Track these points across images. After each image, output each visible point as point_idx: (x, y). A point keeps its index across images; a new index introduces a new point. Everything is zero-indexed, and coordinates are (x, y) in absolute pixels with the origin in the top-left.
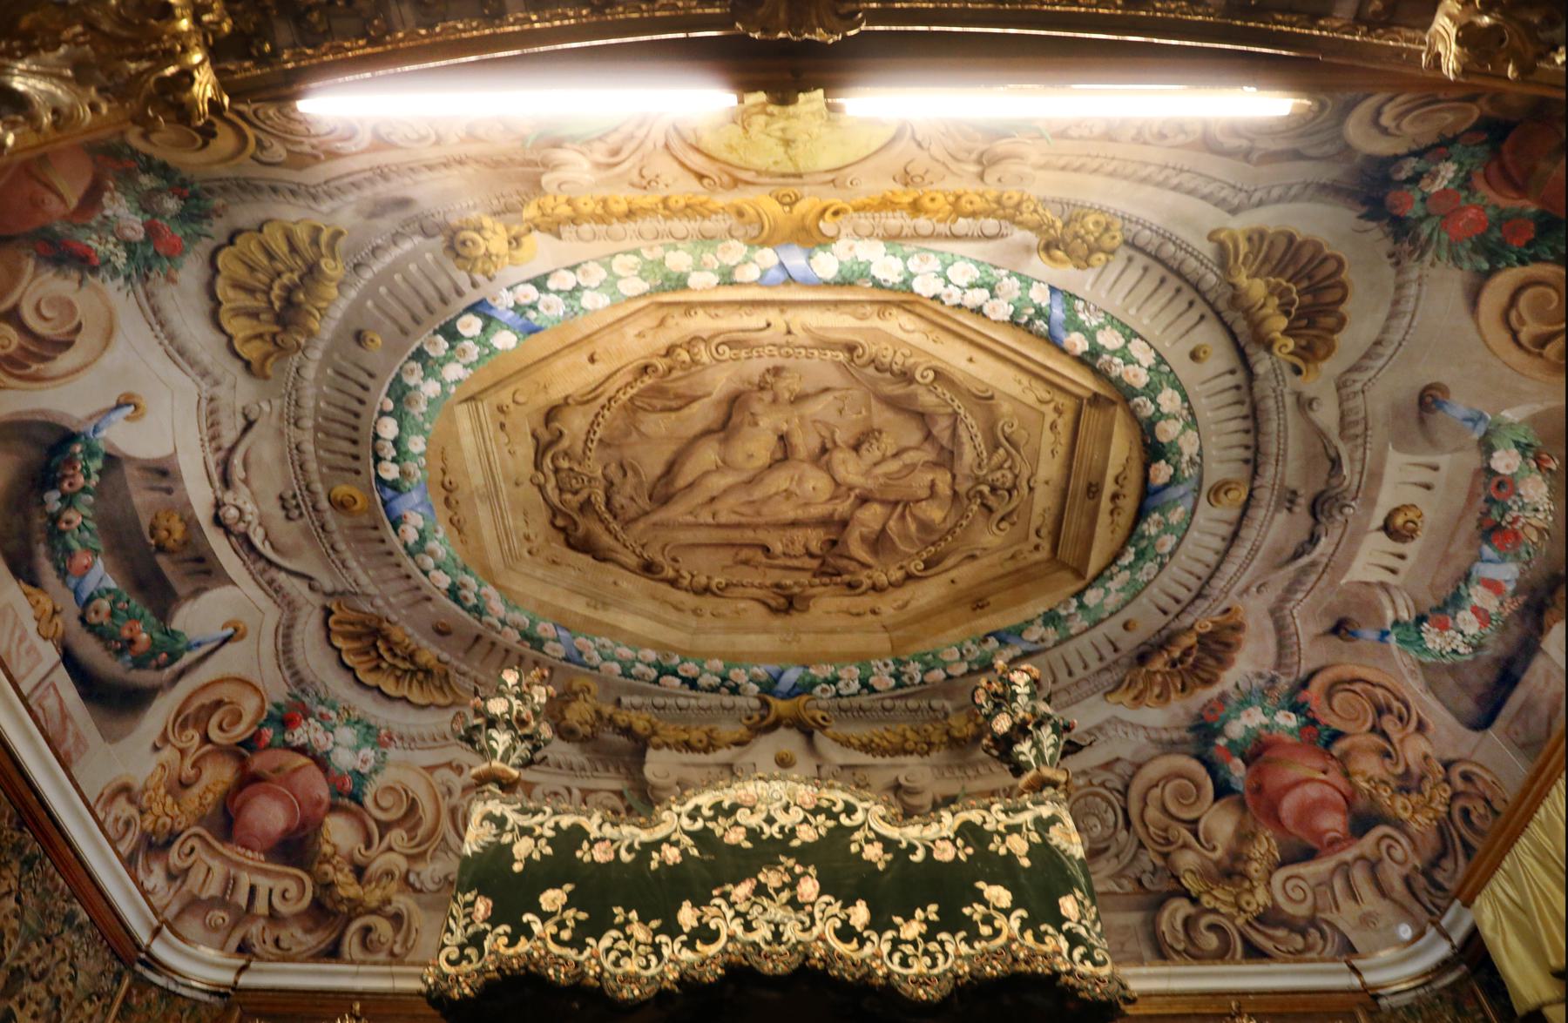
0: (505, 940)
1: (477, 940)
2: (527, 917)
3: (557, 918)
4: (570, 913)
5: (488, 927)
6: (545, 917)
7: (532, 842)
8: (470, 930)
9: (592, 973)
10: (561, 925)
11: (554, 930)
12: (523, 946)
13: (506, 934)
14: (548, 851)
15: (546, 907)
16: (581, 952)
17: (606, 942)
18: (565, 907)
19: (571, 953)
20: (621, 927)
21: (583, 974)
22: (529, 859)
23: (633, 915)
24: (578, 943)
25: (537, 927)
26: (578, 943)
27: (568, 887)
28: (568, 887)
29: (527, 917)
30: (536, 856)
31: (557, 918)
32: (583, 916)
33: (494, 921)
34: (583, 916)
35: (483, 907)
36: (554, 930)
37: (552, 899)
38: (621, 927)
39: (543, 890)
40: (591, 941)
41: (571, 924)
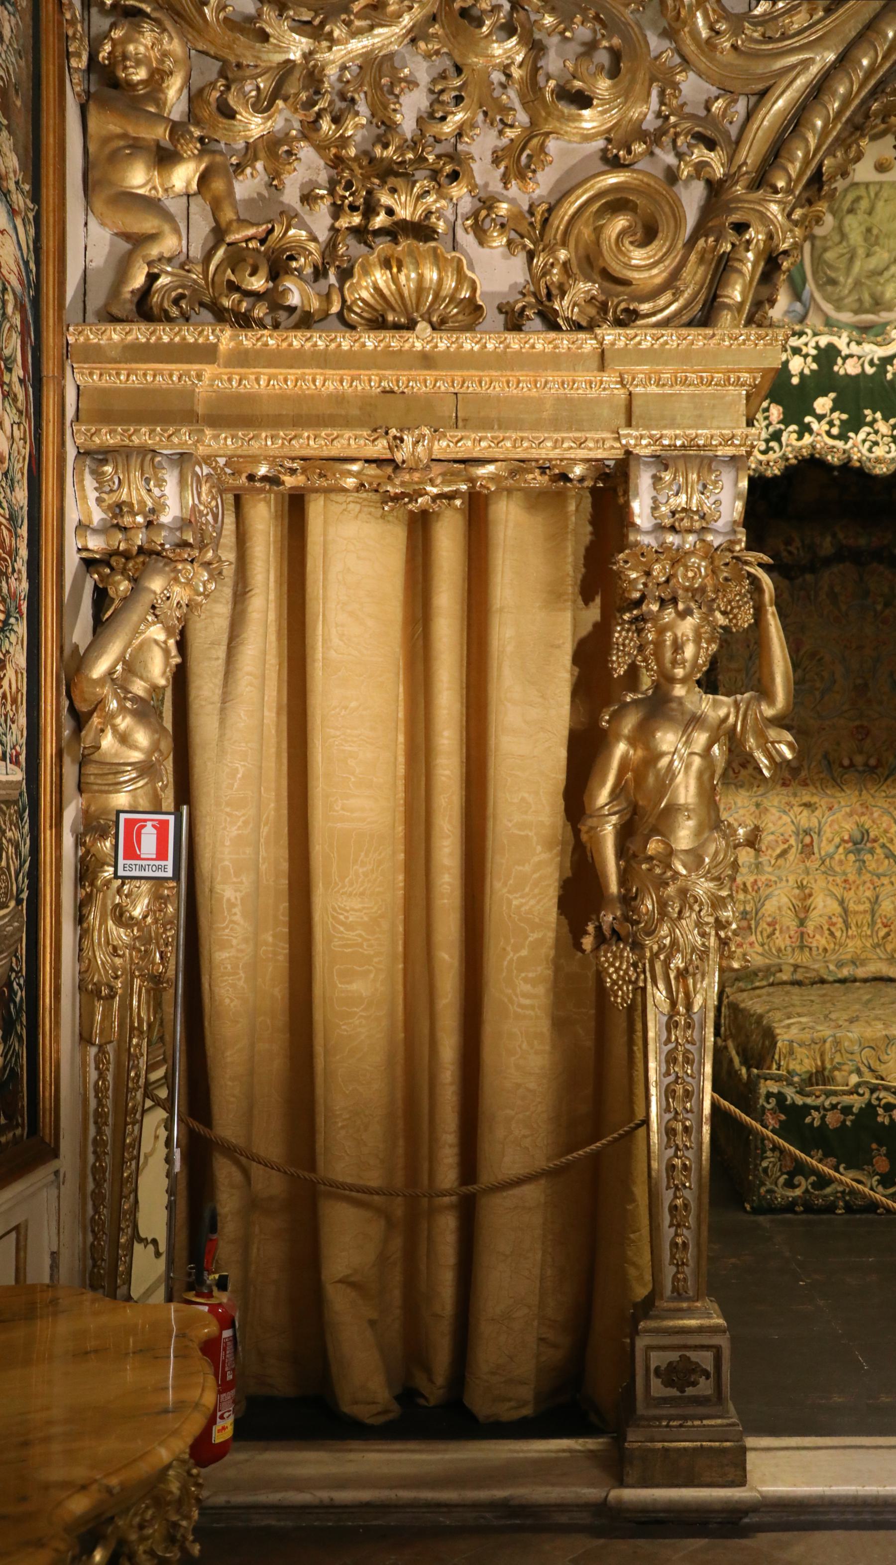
0: (795, 436)
1: (776, 436)
2: (808, 419)
3: (827, 419)
4: (836, 415)
5: (783, 427)
6: (820, 418)
7: (801, 359)
8: (771, 429)
9: (855, 457)
10: (831, 424)
11: (827, 427)
12: (807, 439)
13: (795, 432)
14: (814, 366)
15: (819, 411)
16: (846, 443)
17: (862, 435)
18: (833, 410)
19: (839, 444)
20: (871, 424)
21: (850, 459)
22: (802, 374)
23: (878, 415)
24: (843, 437)
25: (815, 426)
26: (843, 437)
27: (832, 395)
28: (832, 395)
29: (808, 419)
30: (807, 371)
31: (827, 419)
32: (844, 417)
33: (786, 421)
34: (844, 417)
35: (776, 412)
36: (827, 427)
37: (823, 404)
38: (871, 424)
39: (815, 399)
40: (851, 434)
41: (837, 422)
